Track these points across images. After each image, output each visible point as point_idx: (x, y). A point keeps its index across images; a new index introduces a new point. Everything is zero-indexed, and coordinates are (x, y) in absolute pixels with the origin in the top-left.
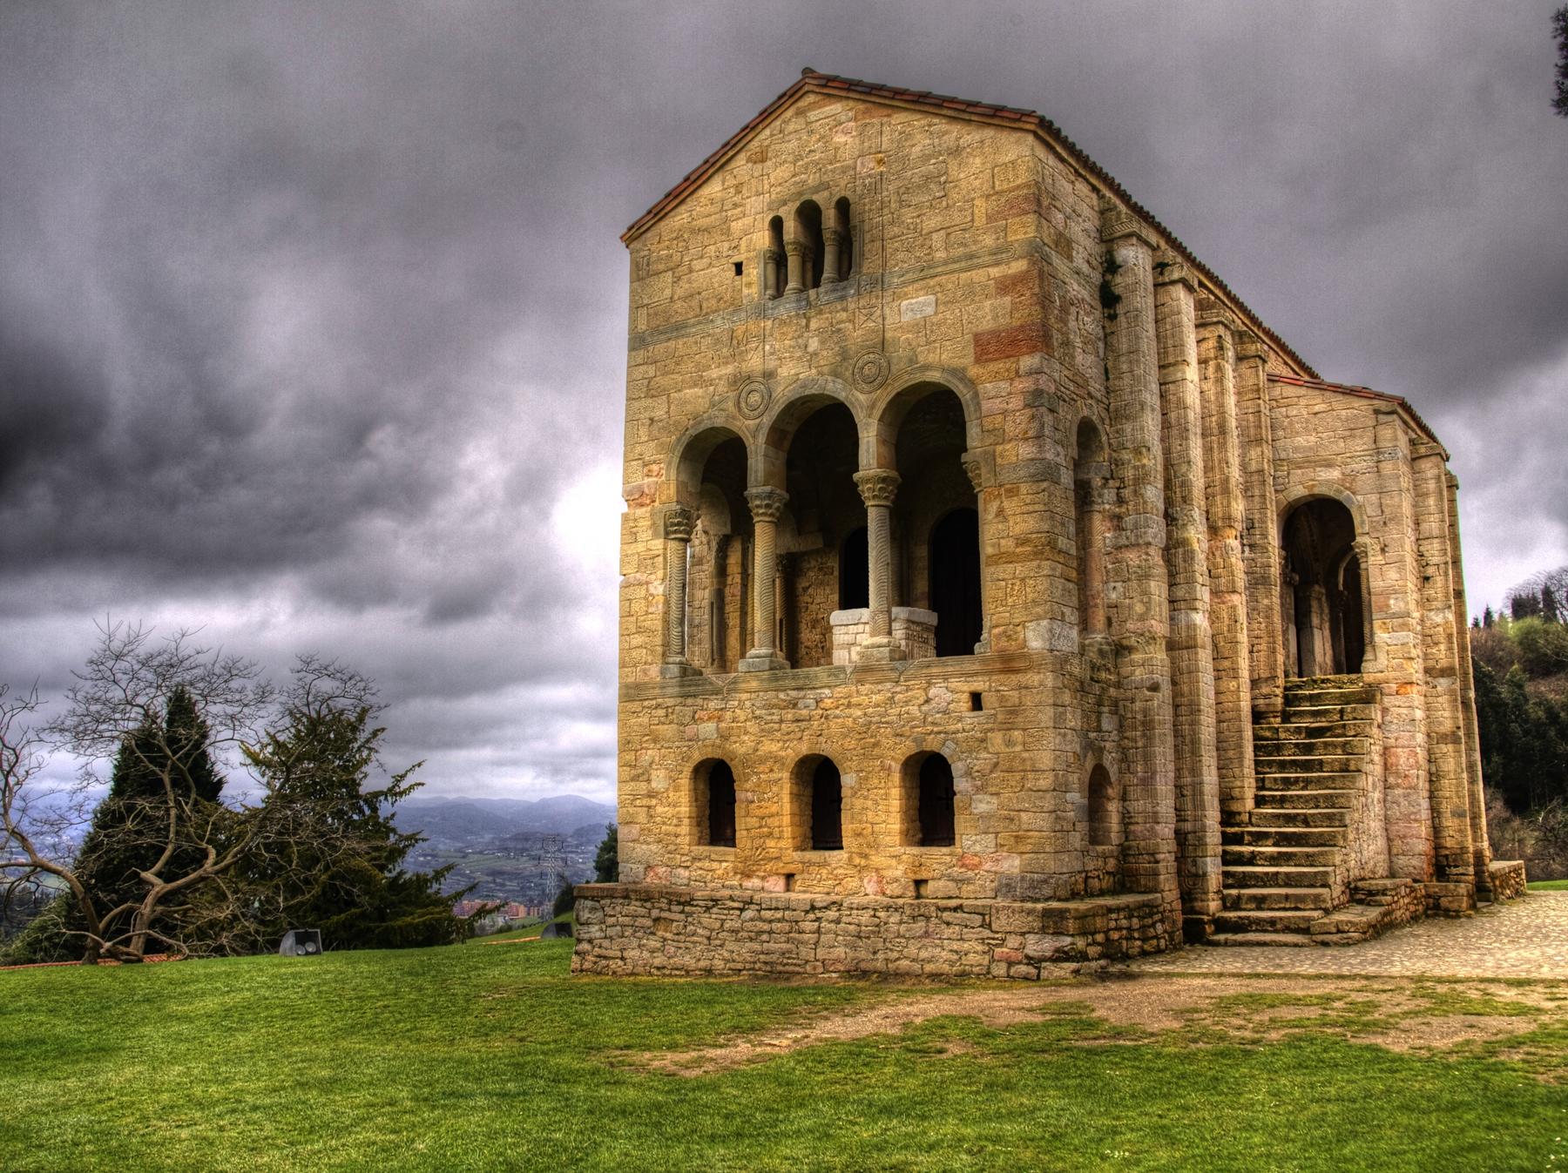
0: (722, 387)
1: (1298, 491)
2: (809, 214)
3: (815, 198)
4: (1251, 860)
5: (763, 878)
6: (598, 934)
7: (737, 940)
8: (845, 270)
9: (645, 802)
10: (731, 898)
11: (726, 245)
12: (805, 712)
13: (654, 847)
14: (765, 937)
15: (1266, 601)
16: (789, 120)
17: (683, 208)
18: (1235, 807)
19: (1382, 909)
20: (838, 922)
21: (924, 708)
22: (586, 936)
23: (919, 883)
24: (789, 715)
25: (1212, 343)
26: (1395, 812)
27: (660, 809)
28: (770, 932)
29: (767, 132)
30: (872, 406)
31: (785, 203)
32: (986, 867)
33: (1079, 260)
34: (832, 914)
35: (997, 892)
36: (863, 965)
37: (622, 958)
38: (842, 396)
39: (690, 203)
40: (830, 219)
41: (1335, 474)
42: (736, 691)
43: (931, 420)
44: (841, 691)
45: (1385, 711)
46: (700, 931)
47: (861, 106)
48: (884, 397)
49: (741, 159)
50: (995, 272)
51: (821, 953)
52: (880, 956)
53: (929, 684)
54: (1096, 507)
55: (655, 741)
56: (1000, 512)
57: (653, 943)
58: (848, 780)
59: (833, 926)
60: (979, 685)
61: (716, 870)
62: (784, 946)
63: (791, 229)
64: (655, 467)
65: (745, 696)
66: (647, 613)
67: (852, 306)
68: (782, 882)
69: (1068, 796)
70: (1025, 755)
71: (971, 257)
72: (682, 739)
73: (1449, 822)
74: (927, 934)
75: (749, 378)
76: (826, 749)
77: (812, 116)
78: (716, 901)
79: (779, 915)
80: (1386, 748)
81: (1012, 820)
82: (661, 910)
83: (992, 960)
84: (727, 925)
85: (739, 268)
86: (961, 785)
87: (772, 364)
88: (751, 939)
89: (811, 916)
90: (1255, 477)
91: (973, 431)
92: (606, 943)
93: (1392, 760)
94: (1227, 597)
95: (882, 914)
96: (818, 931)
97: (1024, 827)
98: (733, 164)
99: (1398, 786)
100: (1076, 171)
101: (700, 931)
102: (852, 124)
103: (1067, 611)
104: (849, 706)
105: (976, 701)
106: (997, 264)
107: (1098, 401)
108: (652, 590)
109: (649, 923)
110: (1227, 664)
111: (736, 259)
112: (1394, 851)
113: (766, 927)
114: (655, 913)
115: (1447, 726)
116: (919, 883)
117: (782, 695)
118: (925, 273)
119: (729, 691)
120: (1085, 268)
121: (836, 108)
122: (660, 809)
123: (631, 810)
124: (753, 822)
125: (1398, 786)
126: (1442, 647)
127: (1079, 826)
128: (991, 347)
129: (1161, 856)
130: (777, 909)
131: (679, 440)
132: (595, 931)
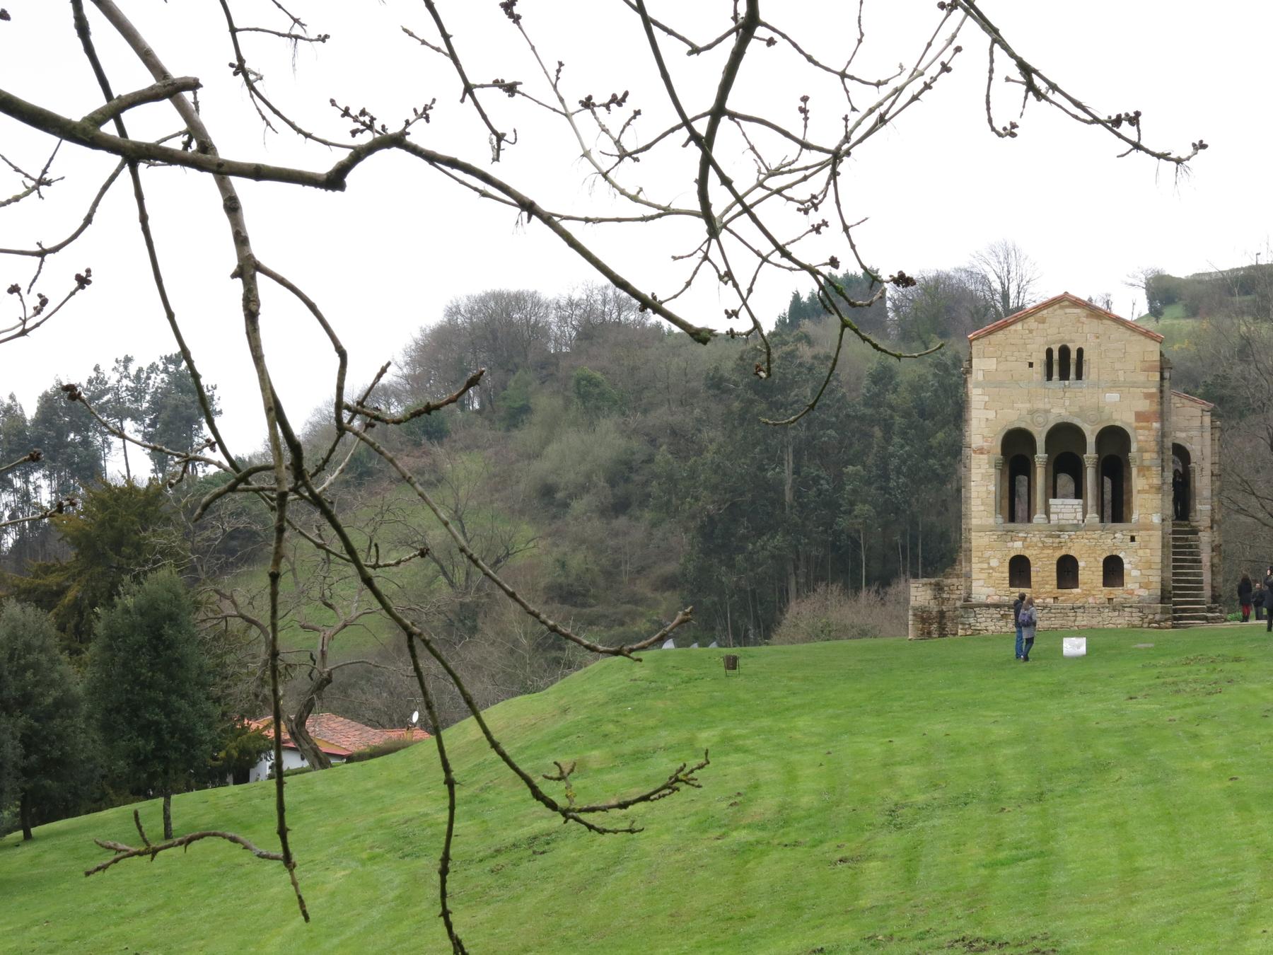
0: (1024, 412)
2: (1064, 351)
8: (1079, 376)
16: (1057, 311)
30: (1093, 431)
39: (1006, 331)
40: (1074, 355)
41: (1183, 435)
43: (1114, 438)
48: (1099, 428)
49: (1031, 320)
57: (1001, 623)
58: (1081, 564)
63: (1056, 355)
67: (1085, 391)
75: (1037, 411)
77: (1068, 310)
85: (1031, 365)
86: (1126, 566)
87: (1048, 407)
91: (1134, 447)
105: (1133, 539)
118: (1115, 386)
121: (1078, 311)
128: (1140, 416)
132: (972, 621)
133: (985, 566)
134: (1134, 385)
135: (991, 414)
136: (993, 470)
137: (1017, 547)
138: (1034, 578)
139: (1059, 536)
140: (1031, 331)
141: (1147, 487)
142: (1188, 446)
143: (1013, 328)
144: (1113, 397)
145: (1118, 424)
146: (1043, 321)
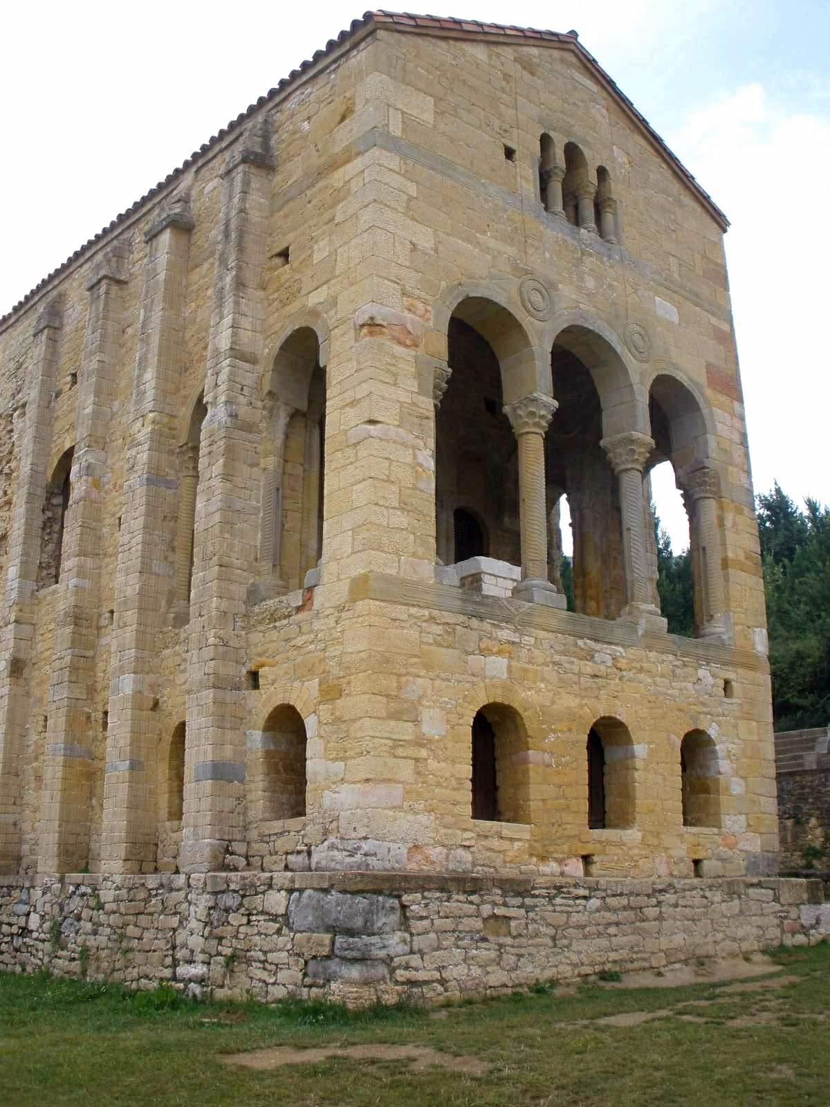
3: (580, 146)
5: (560, 862)
6: (401, 948)
7: (585, 937)
9: (411, 752)
10: (576, 886)
11: (497, 123)
12: (602, 668)
13: (423, 818)
14: (612, 930)
17: (443, 44)
20: (676, 906)
21: (697, 687)
22: (382, 954)
23: (697, 862)
24: (588, 668)
27: (432, 764)
28: (617, 924)
29: (535, 51)
31: (554, 130)
32: (740, 846)
34: (669, 898)
35: (747, 869)
36: (698, 952)
37: (442, 982)
38: (619, 350)
42: (530, 624)
44: (632, 652)
46: (543, 929)
47: (613, 105)
49: (508, 53)
50: (714, 320)
51: (664, 943)
52: (710, 939)
55: (428, 667)
56: (735, 524)
57: (486, 953)
58: (640, 750)
59: (671, 909)
60: (730, 675)
61: (505, 846)
62: (632, 938)
64: (421, 306)
65: (542, 634)
66: (415, 488)
68: (581, 865)
70: (760, 744)
71: (697, 295)
72: (464, 672)
74: (741, 912)
76: (622, 714)
78: (559, 888)
79: (624, 901)
81: (754, 802)
82: (494, 904)
83: (783, 932)
84: (575, 918)
88: (599, 935)
89: (654, 901)
92: (415, 960)
95: (708, 894)
96: (660, 918)
97: (762, 810)
98: (500, 50)
101: (543, 929)
102: (604, 111)
104: (641, 670)
106: (713, 314)
108: (421, 459)
109: (479, 924)
111: (510, 144)
113: (614, 918)
114: (486, 910)
117: (580, 643)
118: (669, 288)
119: (524, 623)
122: (432, 764)
123: (391, 761)
124: (550, 790)
130: (621, 894)
131: (450, 289)
132: (395, 942)
133: (406, 731)
134: (696, 299)
135: (425, 240)
136: (428, 406)
137: (493, 675)
139: (590, 656)
140: (507, 77)
141: (742, 557)
143: (469, 48)
144: (665, 309)
145: (681, 377)
146: (529, 67)
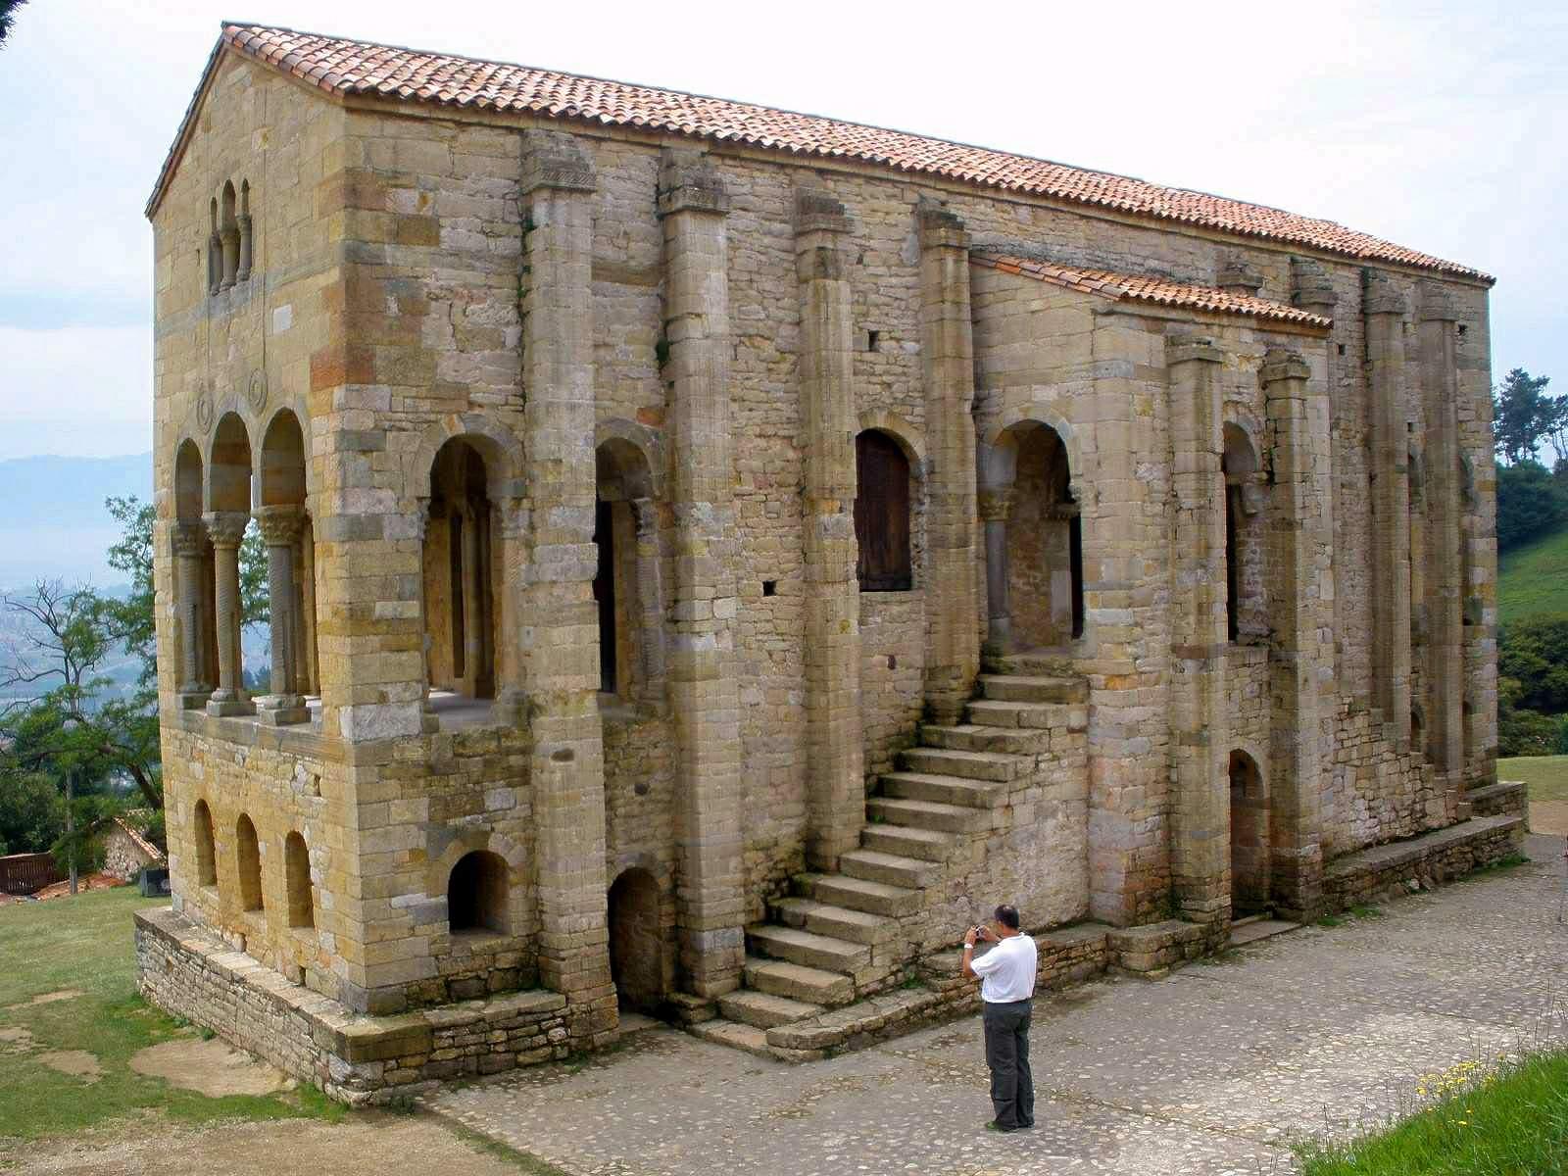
1: (1013, 415)
4: (802, 924)
15: (944, 569)
18: (822, 849)
19: (929, 997)
21: (294, 784)
25: (810, 258)
26: (1096, 840)
33: (458, 234)
41: (1046, 394)
45: (1090, 711)
53: (295, 760)
54: (508, 534)
69: (395, 901)
73: (1187, 845)
80: (1090, 758)
90: (938, 406)
93: (1097, 772)
94: (821, 589)
99: (1101, 805)
100: (454, 122)
103: (392, 691)
107: (494, 406)
110: (816, 674)
112: (1094, 885)
115: (1190, 724)
116: (303, 970)
120: (476, 242)
125: (1101, 805)
126: (1192, 619)
127: (420, 929)
129: (563, 954)
138: (220, 873)
142: (1060, 424)
